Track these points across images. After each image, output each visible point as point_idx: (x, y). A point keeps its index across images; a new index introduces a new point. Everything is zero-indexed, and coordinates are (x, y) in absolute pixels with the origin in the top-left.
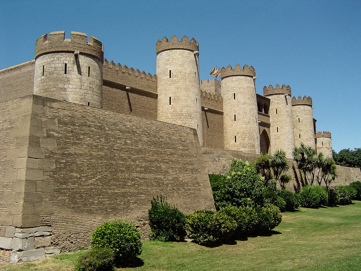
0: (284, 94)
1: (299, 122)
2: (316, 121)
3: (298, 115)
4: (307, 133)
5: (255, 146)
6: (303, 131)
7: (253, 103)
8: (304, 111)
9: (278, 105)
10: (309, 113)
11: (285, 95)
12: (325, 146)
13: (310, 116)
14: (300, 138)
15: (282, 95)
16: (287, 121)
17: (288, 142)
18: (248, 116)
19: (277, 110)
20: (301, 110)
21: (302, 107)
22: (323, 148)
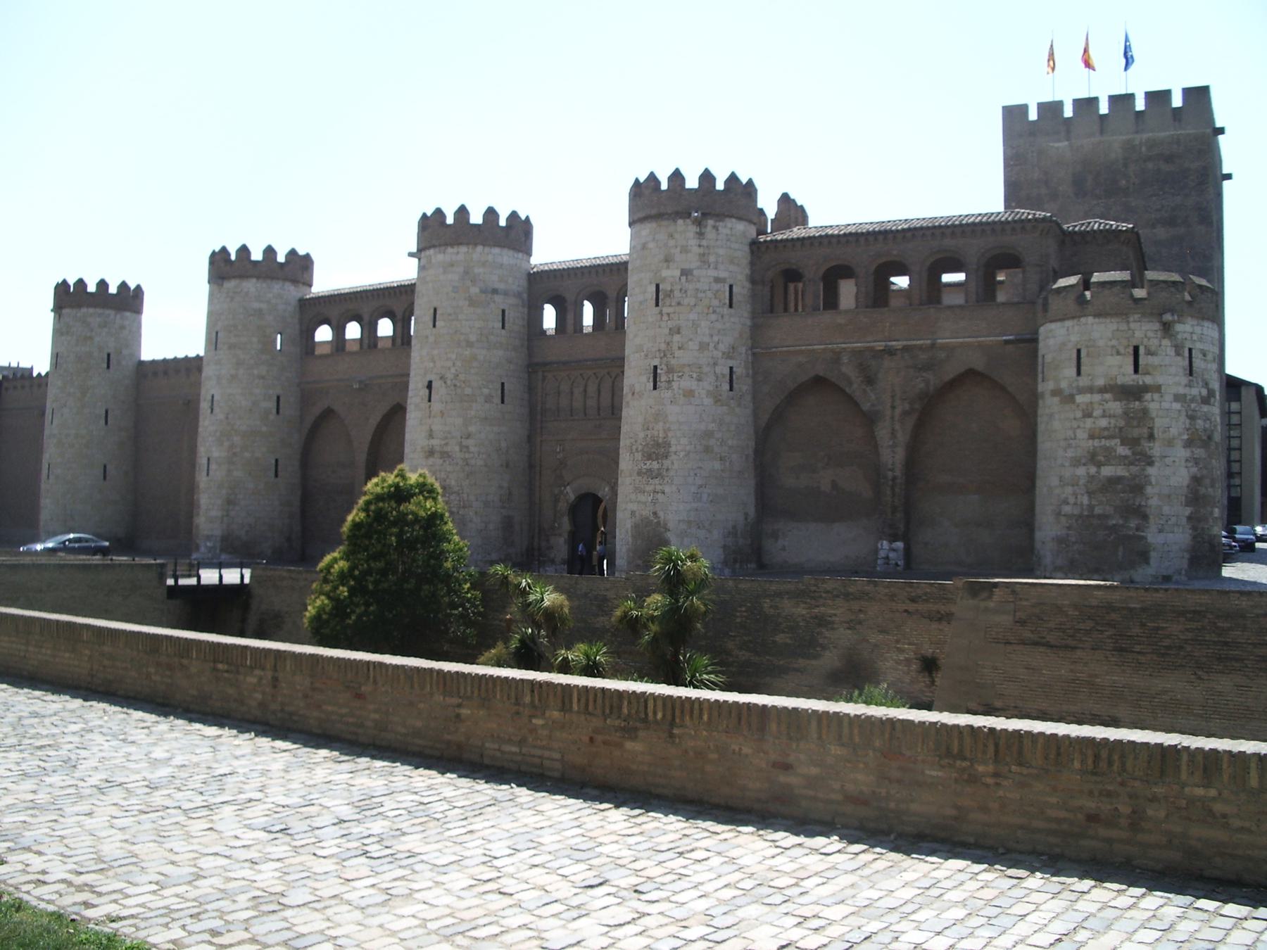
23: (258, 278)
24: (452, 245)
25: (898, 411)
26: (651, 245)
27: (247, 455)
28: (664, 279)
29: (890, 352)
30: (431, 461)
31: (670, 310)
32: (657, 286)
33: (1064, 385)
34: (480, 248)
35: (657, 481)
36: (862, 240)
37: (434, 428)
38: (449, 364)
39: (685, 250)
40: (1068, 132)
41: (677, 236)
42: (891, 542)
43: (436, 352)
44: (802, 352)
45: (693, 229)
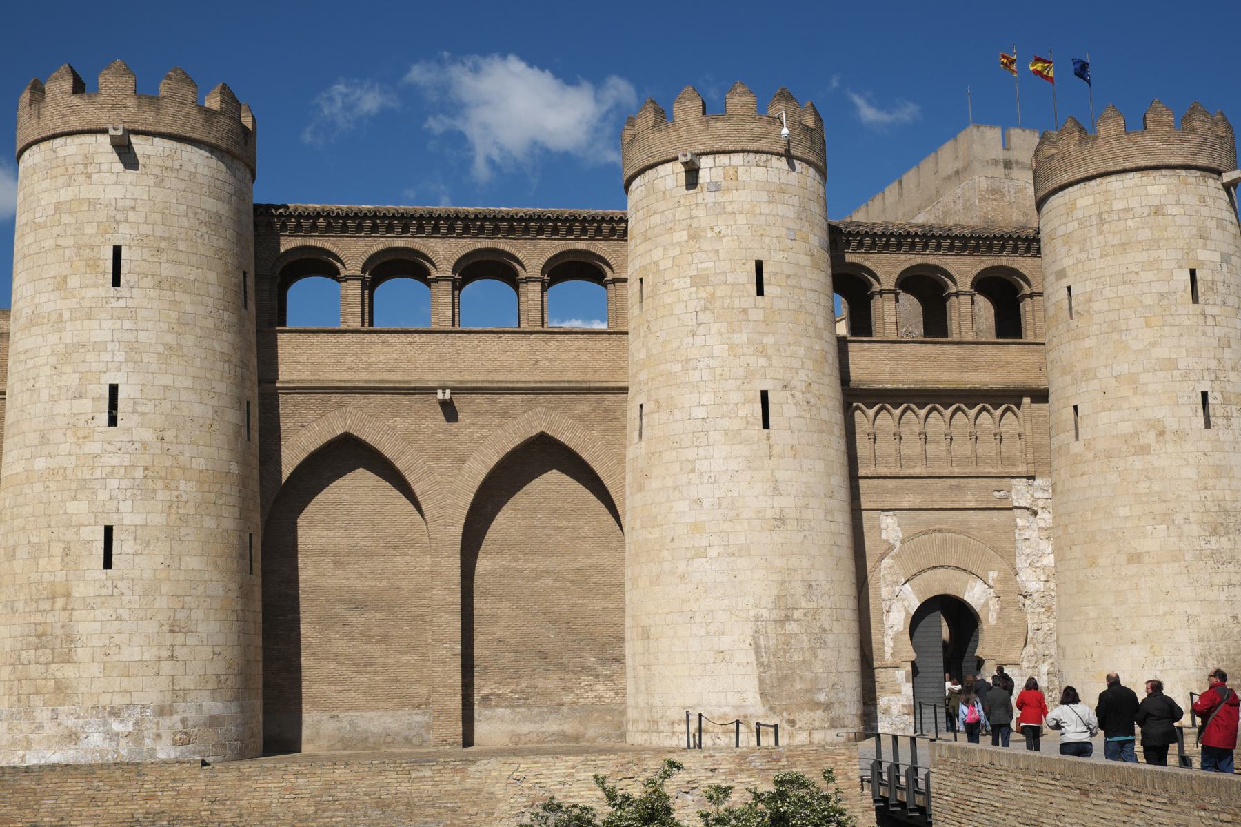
0: (677, 159)
3: (1067, 262)
4: (1125, 391)
5: (68, 595)
6: (1094, 385)
7: (86, 303)
8: (1102, 221)
10: (1145, 234)
13: (1162, 254)
15: (669, 166)
16: (693, 353)
17: (699, 501)
18: (45, 395)
20: (1081, 223)
21: (1083, 198)
23: (212, 149)
27: (210, 523)
28: (1203, 262)
31: (1215, 311)
32: (1193, 273)
34: (812, 170)
37: (781, 475)
38: (796, 363)
39: (1221, 226)
41: (1210, 202)
43: (769, 340)
45: (1223, 194)
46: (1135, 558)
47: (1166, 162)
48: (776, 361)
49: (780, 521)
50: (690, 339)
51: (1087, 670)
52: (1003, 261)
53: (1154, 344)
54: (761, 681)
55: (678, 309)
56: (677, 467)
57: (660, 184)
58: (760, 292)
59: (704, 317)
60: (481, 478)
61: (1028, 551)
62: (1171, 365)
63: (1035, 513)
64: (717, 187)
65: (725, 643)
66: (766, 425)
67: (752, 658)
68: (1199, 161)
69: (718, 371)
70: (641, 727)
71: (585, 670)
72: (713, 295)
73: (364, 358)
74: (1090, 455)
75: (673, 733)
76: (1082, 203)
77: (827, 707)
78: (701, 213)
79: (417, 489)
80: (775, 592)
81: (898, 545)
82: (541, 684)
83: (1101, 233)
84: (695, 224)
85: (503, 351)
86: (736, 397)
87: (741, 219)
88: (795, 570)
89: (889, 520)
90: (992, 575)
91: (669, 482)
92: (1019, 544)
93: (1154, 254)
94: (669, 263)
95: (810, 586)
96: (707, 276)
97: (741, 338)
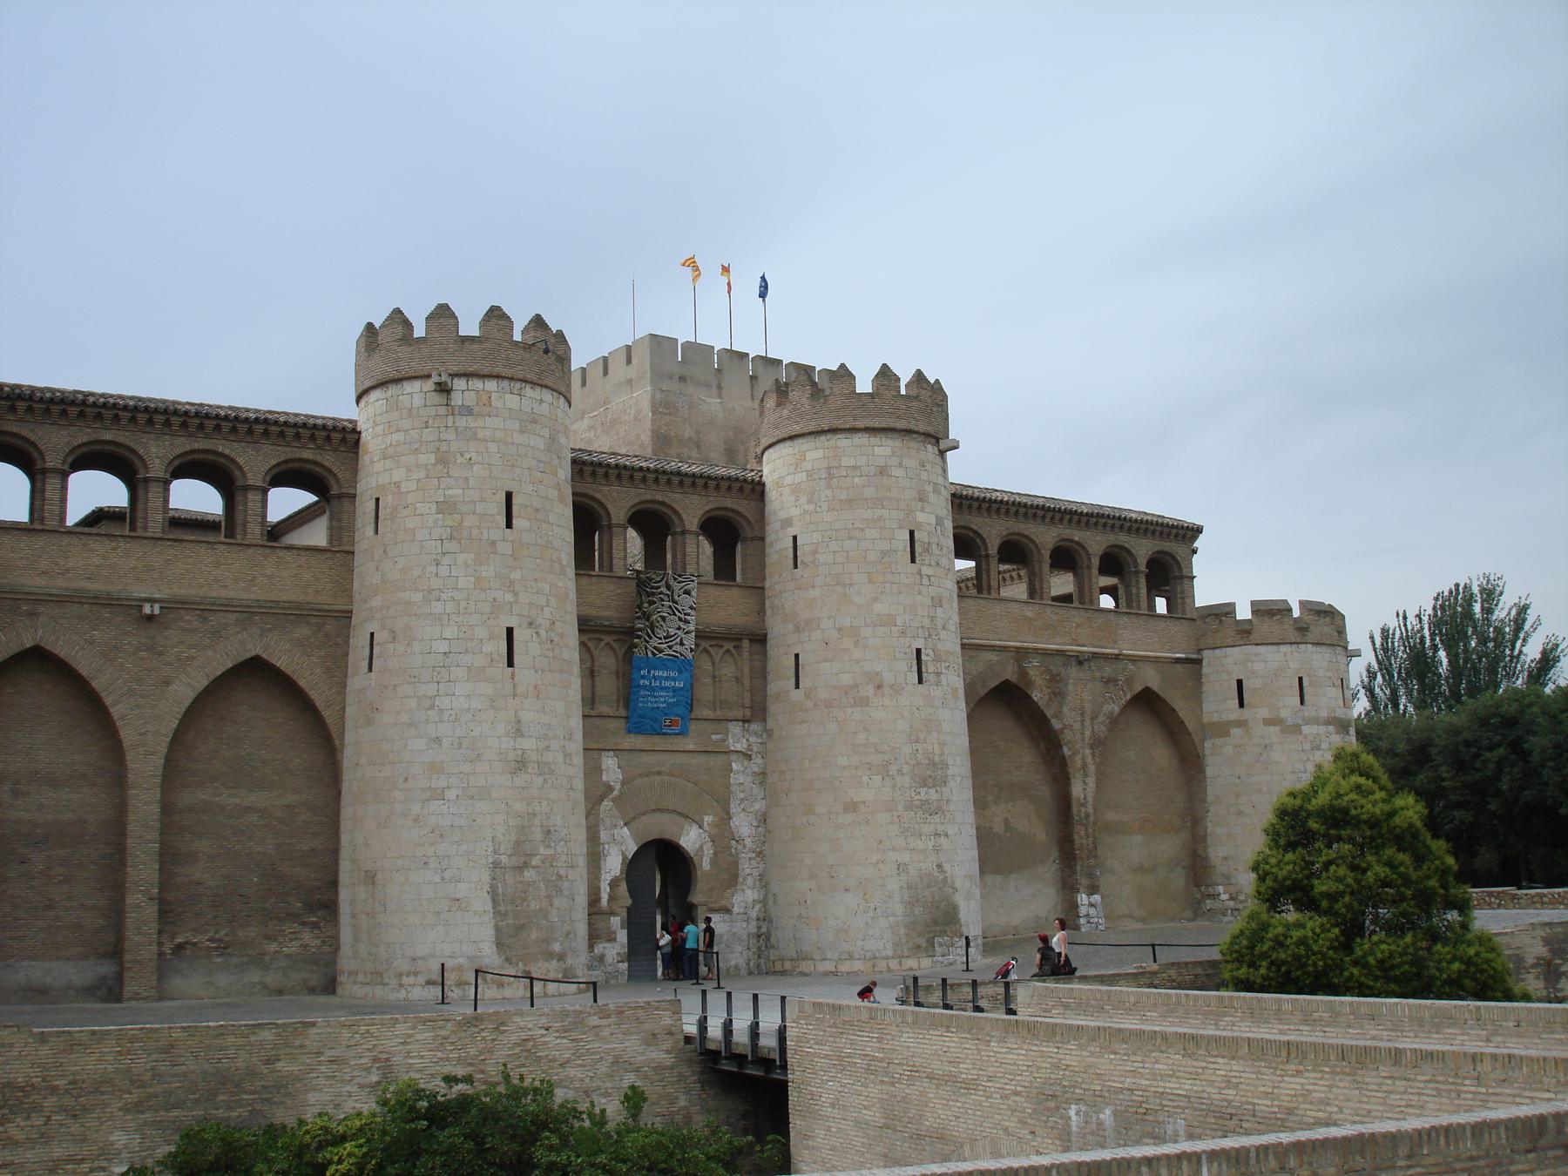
0: (429, 376)
1: (796, 567)
2: (1188, 534)
3: (794, 512)
6: (817, 635)
9: (388, 464)
10: (870, 492)
11: (435, 379)
12: (1257, 712)
13: (884, 512)
14: (797, 687)
15: (416, 385)
16: (436, 583)
17: (438, 740)
19: (377, 500)
21: (814, 452)
22: (1242, 724)
24: (533, 384)
25: (1088, 733)
26: (897, 472)
28: (920, 524)
29: (1080, 660)
30: (520, 780)
32: (912, 533)
33: (1284, 714)
35: (937, 818)
36: (1049, 515)
37: (525, 716)
38: (543, 601)
40: (720, 387)
41: (928, 467)
42: (1090, 894)
43: (517, 575)
44: (992, 648)
46: (851, 807)
47: (892, 425)
48: (523, 597)
49: (521, 764)
50: (434, 569)
51: (800, 917)
52: (729, 503)
53: (875, 600)
54: (498, 930)
55: (422, 535)
56: (413, 703)
57: (405, 400)
58: (509, 525)
59: (449, 546)
60: (187, 703)
61: (742, 796)
62: (890, 620)
63: (750, 757)
64: (468, 411)
65: (462, 890)
66: (510, 663)
67: (489, 907)
68: (921, 427)
69: (463, 604)
70: (361, 978)
71: (291, 916)
72: (460, 524)
73: (61, 562)
74: (810, 704)
75: (401, 986)
76: (811, 455)
77: (561, 957)
78: (451, 436)
79: (116, 712)
80: (514, 837)
81: (618, 787)
82: (241, 933)
83: (829, 487)
84: (444, 447)
85: (218, 565)
86: (481, 633)
87: (493, 447)
88: (534, 814)
89: (610, 762)
90: (708, 819)
91: (405, 718)
92: (733, 789)
93: (879, 512)
94: (413, 485)
95: (549, 832)
96: (455, 504)
97: (488, 571)
